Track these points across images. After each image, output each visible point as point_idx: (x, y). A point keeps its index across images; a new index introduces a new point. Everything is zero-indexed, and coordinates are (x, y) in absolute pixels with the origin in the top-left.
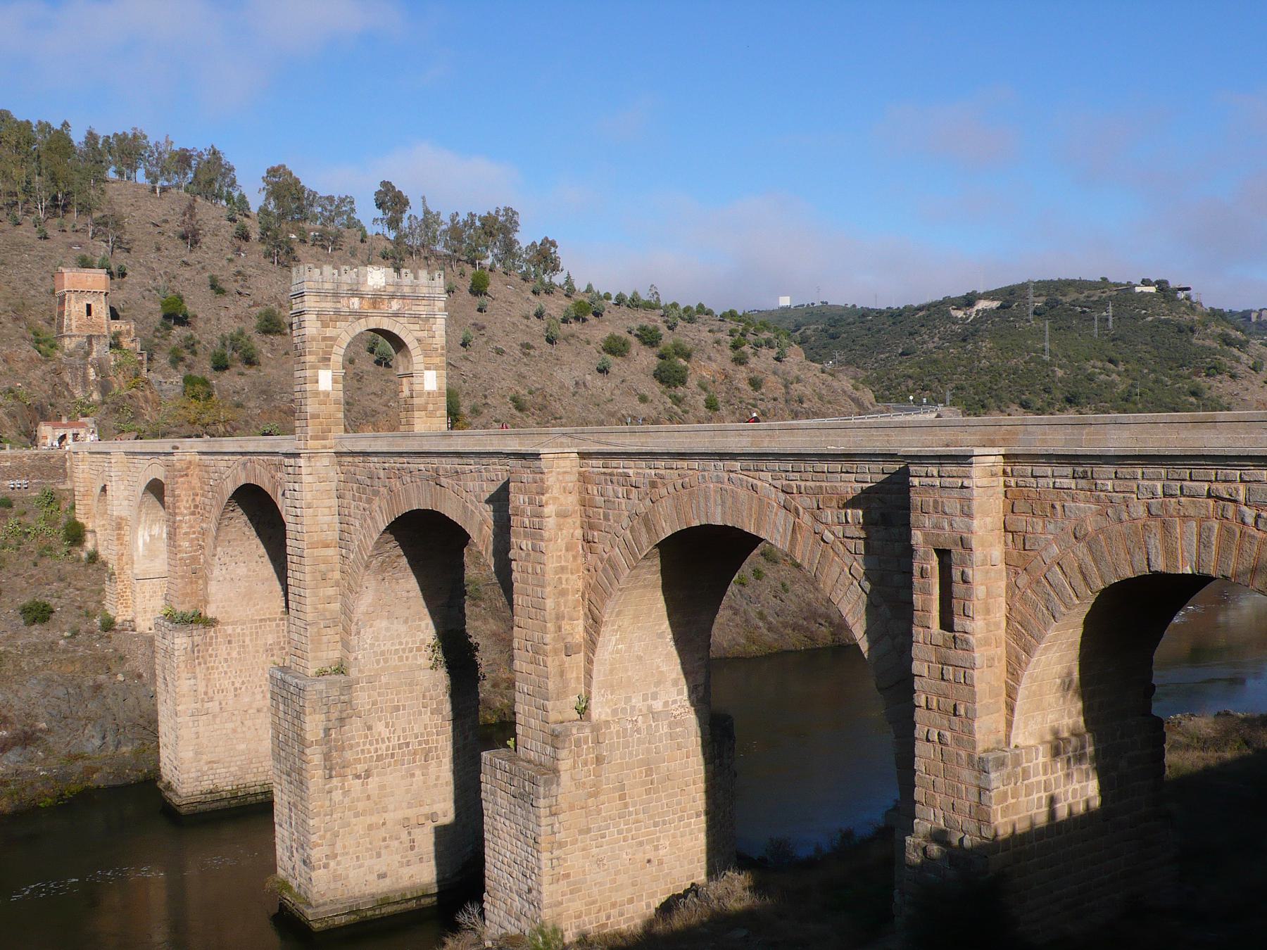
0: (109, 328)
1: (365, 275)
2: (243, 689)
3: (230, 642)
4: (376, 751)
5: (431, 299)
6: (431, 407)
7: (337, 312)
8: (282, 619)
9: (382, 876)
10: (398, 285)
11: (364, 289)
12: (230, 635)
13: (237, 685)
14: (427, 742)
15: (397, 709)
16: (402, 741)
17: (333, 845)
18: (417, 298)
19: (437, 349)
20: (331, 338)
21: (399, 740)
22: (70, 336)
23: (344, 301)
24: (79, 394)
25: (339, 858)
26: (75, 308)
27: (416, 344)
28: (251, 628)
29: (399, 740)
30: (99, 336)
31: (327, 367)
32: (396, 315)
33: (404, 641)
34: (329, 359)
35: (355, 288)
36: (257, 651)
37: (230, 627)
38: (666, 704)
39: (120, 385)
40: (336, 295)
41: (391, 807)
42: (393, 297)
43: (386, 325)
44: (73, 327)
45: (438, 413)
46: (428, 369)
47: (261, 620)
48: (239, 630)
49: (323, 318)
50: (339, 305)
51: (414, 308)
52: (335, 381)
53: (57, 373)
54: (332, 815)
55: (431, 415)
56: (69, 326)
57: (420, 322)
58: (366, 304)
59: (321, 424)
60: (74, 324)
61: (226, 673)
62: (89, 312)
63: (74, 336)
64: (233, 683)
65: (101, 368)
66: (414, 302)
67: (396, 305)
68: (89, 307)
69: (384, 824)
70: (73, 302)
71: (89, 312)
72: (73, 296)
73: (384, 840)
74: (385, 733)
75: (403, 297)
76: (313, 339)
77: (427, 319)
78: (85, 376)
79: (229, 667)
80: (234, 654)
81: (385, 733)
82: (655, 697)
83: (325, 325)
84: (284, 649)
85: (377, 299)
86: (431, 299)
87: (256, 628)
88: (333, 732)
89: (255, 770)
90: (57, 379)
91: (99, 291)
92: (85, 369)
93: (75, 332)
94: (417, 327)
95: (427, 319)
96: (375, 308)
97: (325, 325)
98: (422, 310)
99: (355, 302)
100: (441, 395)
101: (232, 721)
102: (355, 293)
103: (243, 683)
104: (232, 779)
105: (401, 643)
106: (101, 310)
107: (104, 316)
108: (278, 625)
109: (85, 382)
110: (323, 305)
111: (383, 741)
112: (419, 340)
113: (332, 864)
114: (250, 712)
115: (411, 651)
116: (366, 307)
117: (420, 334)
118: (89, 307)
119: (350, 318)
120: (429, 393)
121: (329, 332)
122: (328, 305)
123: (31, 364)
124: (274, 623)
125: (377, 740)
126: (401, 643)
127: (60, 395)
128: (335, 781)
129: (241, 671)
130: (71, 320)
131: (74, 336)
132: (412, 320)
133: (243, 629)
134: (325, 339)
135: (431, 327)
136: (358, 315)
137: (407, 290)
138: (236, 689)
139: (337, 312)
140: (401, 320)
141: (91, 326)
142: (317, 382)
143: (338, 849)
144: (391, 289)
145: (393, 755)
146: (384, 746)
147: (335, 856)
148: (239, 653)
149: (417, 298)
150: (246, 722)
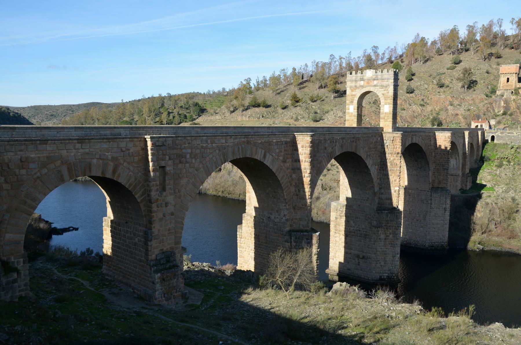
0: (516, 86)
1: (366, 73)
2: (412, 212)
3: (410, 195)
4: (349, 229)
5: (388, 79)
6: (386, 118)
7: (356, 86)
8: (428, 191)
9: (349, 269)
10: (377, 76)
11: (365, 78)
12: (410, 193)
13: (411, 210)
14: (366, 232)
15: (357, 218)
16: (358, 229)
17: (336, 254)
18: (382, 79)
19: (389, 97)
20: (354, 95)
21: (357, 228)
22: (498, 90)
23: (358, 82)
24: (496, 111)
25: (337, 258)
26: (503, 79)
27: (382, 95)
28: (417, 192)
29: (357, 228)
30: (507, 90)
31: (352, 104)
32: (375, 86)
33: (362, 196)
34: (353, 102)
35: (362, 78)
36: (419, 200)
37: (410, 190)
38: (275, 217)
39: (513, 107)
40: (356, 81)
41: (353, 249)
42: (374, 80)
43: (371, 89)
44: (501, 87)
45: (389, 120)
46: (385, 104)
47: (421, 190)
48: (413, 192)
49: (352, 88)
50: (356, 84)
51: (382, 83)
52: (354, 109)
53: (491, 104)
54: (336, 244)
55: (386, 121)
56: (500, 86)
57: (384, 88)
58: (365, 83)
59: (350, 123)
60: (501, 85)
61: (408, 205)
62: (508, 81)
63: (500, 90)
64: (410, 209)
65: (506, 102)
66: (382, 81)
67: (375, 82)
68: (508, 79)
69: (350, 253)
70: (502, 77)
71: (508, 81)
72: (502, 75)
73: (350, 258)
74: (353, 225)
75: (377, 79)
76: (348, 96)
77: (386, 87)
78: (500, 104)
79: (409, 203)
80: (411, 200)
81: (353, 225)
82: (271, 214)
83: (352, 91)
84: (428, 201)
85: (369, 80)
86: (388, 79)
87: (419, 192)
88: (338, 219)
89: (414, 240)
90: (489, 106)
91: (512, 73)
92: (500, 102)
93: (501, 88)
94: (383, 89)
95: (386, 87)
96: (368, 84)
97: (352, 91)
98: (385, 83)
99: (362, 83)
100: (390, 114)
101: (408, 221)
102: (362, 79)
103: (413, 210)
104: (406, 240)
105: (361, 197)
106: (514, 79)
107: (514, 82)
108: (426, 193)
109: (499, 106)
110: (352, 84)
111: (352, 227)
112: (383, 94)
113: (335, 259)
114: (414, 220)
115: (364, 200)
116: (365, 84)
117: (384, 92)
118: (508, 79)
119: (360, 88)
120: (386, 113)
121: (354, 93)
122: (353, 84)
123: (482, 100)
124: (425, 192)
125: (350, 226)
126: (361, 197)
127: (489, 111)
128: (337, 235)
129: (412, 206)
130: (500, 84)
131: (500, 90)
132: (381, 87)
133: (414, 192)
134: (352, 95)
135: (388, 89)
136: (362, 87)
137: (379, 77)
138: (410, 211)
139: (356, 86)
140: (377, 87)
141: (508, 86)
142: (349, 109)
143: (337, 255)
144: (374, 77)
145: (354, 233)
146: (352, 229)
147: (336, 257)
148: (412, 200)
149: (382, 79)
150: (413, 223)
